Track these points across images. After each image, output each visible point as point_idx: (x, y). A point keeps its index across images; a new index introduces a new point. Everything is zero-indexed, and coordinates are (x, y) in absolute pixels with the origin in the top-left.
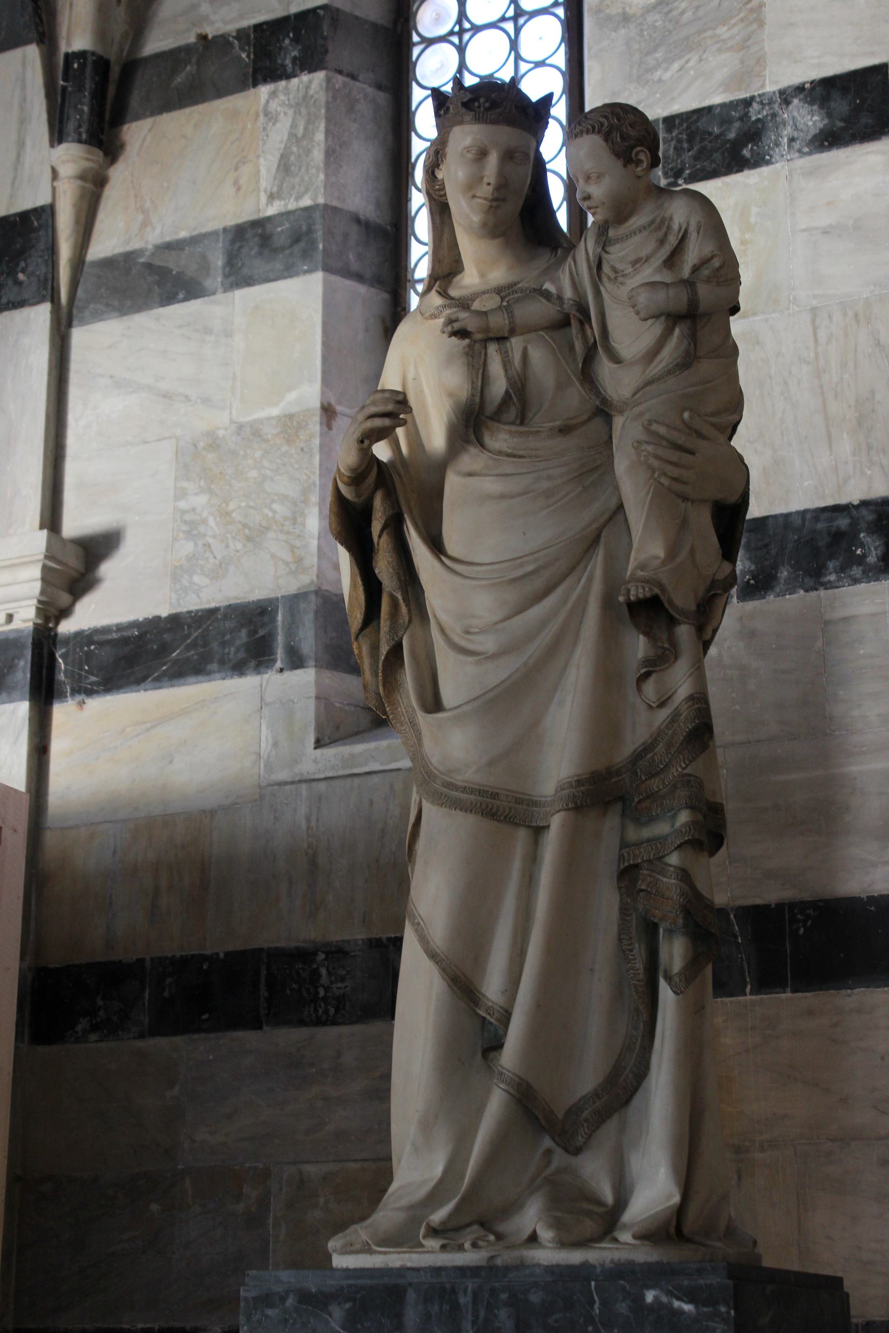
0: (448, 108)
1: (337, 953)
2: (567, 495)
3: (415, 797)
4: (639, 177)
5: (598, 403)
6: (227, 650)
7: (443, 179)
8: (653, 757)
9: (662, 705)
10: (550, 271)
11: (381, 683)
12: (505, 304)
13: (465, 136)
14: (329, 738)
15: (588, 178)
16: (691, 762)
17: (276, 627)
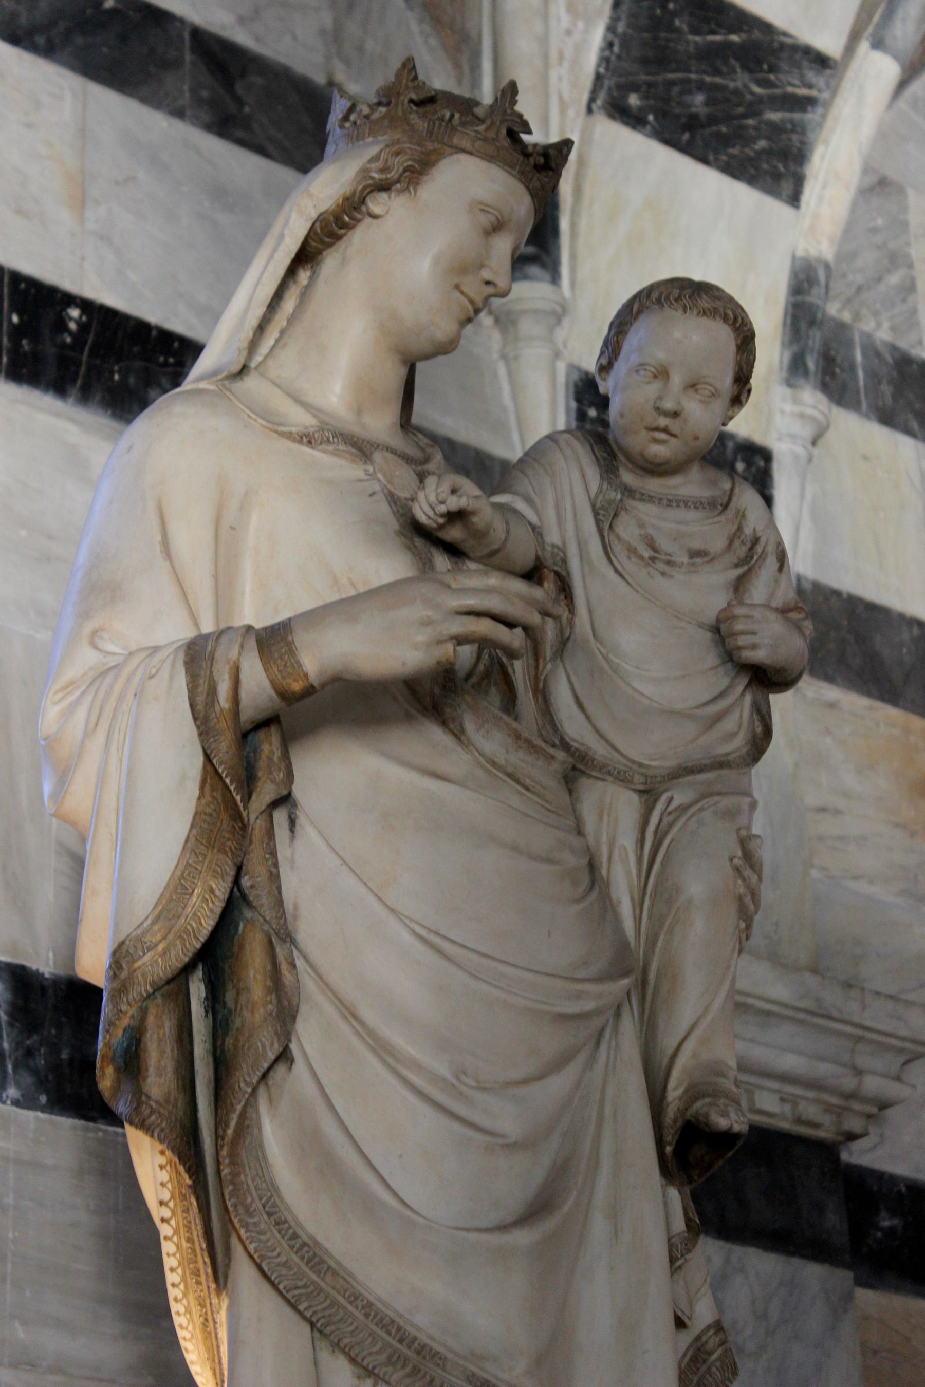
15: (692, 386)
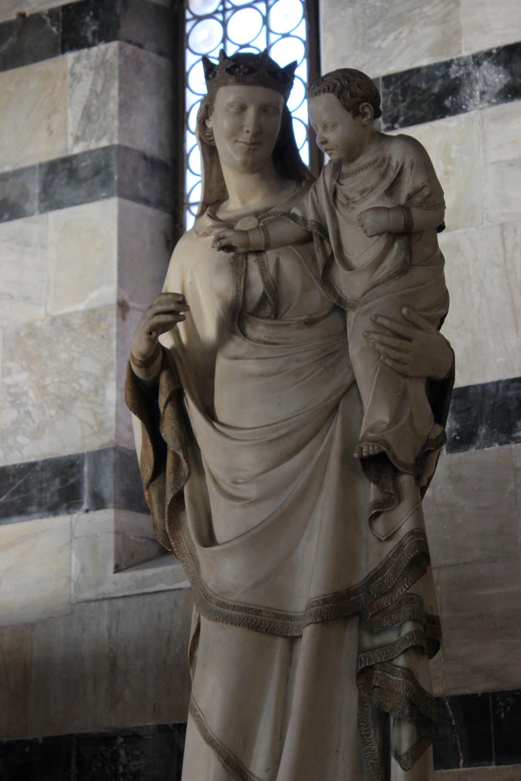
0: (215, 73)
1: (133, 737)
2: (312, 373)
3: (194, 614)
4: (365, 126)
5: (335, 301)
6: (44, 495)
7: (211, 128)
8: (382, 580)
9: (389, 538)
10: (296, 199)
11: (167, 523)
12: (261, 224)
13: (229, 94)
14: (126, 564)
15: (325, 127)
16: (413, 583)
17: (82, 477)
